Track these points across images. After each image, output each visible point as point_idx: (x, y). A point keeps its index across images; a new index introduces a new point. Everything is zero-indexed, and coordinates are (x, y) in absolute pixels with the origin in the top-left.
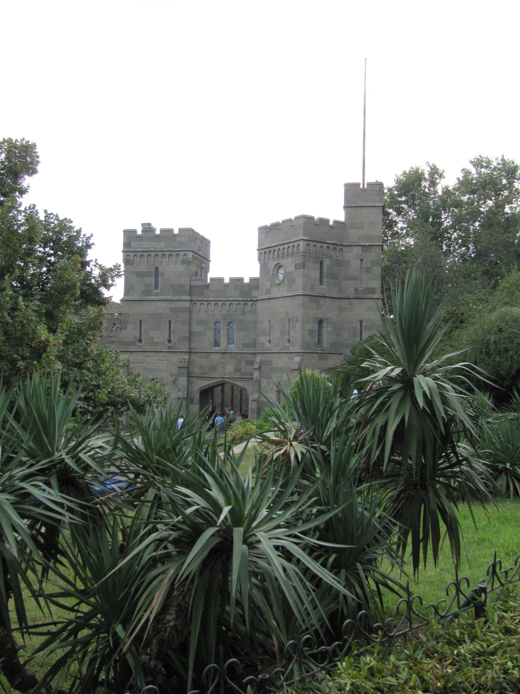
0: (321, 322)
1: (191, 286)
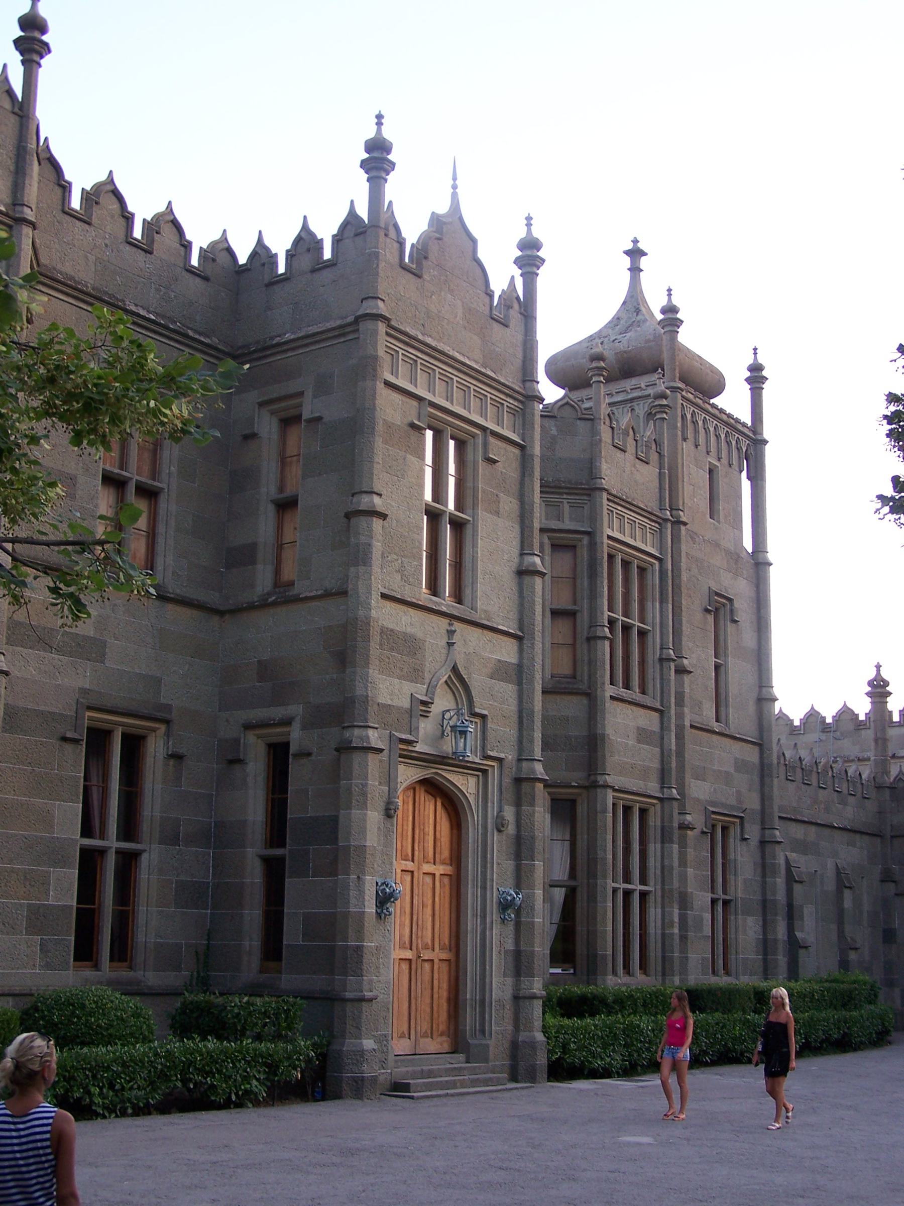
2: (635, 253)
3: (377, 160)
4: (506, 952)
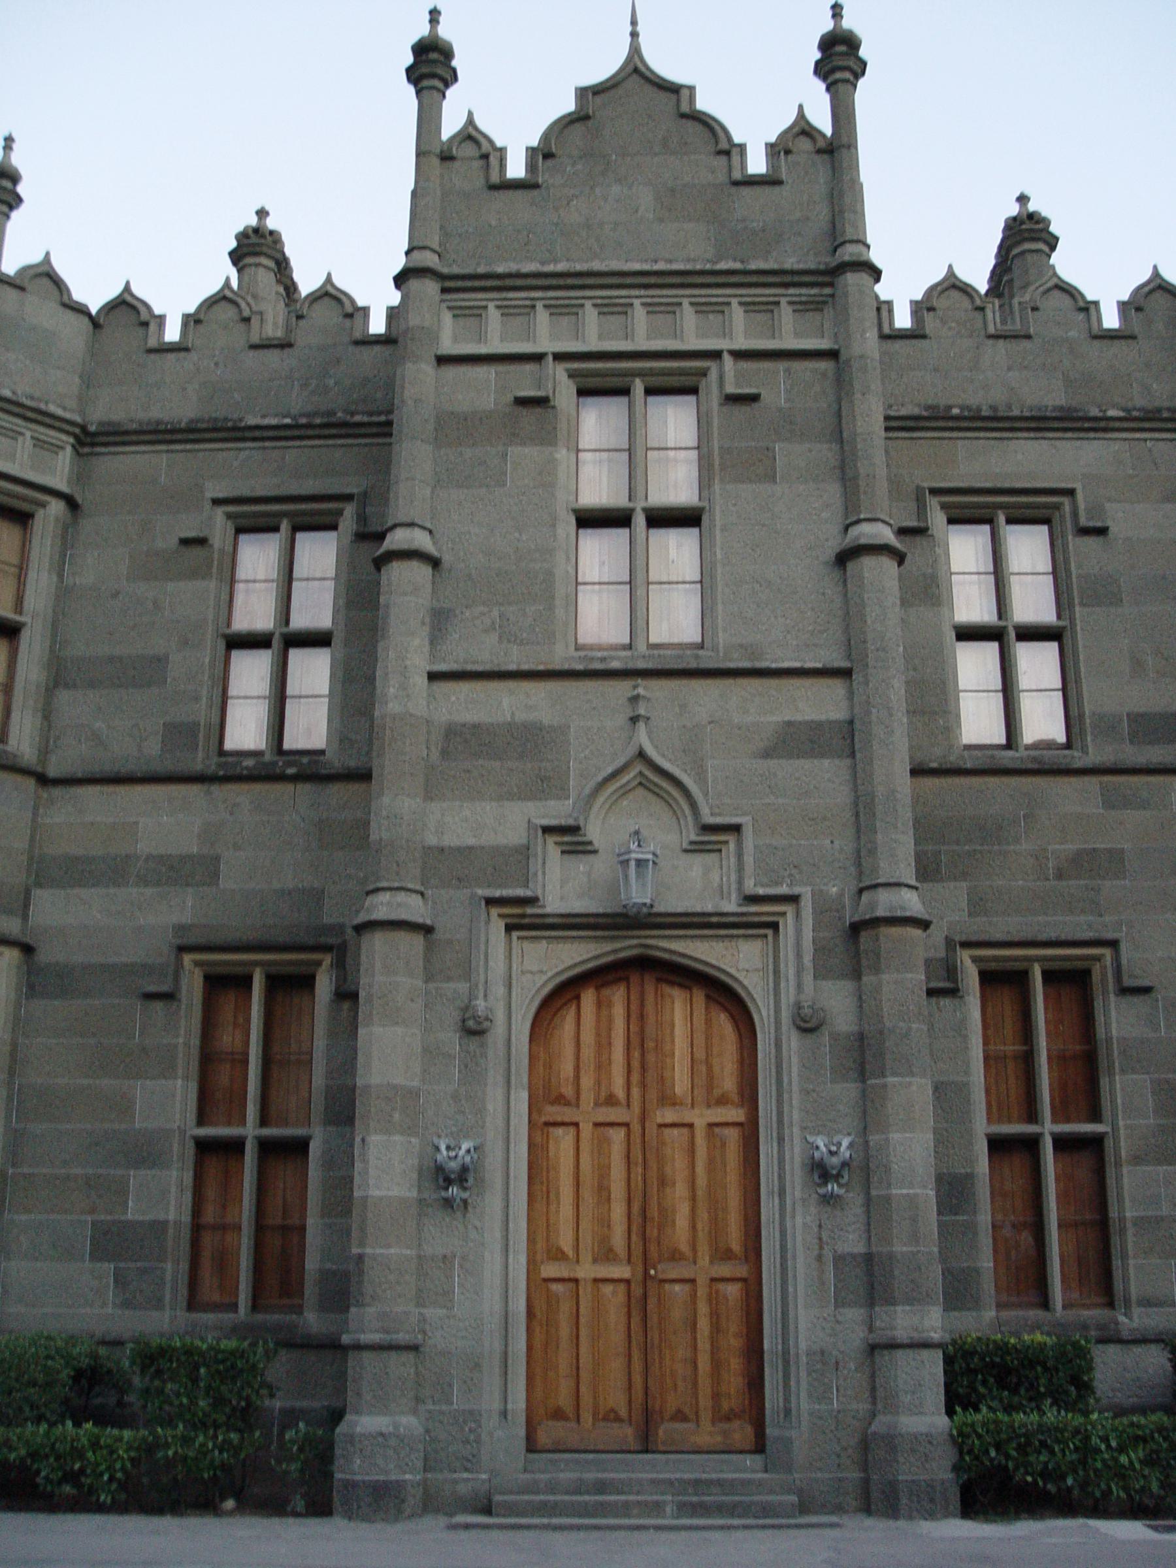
3: (431, 66)
4: (839, 1259)
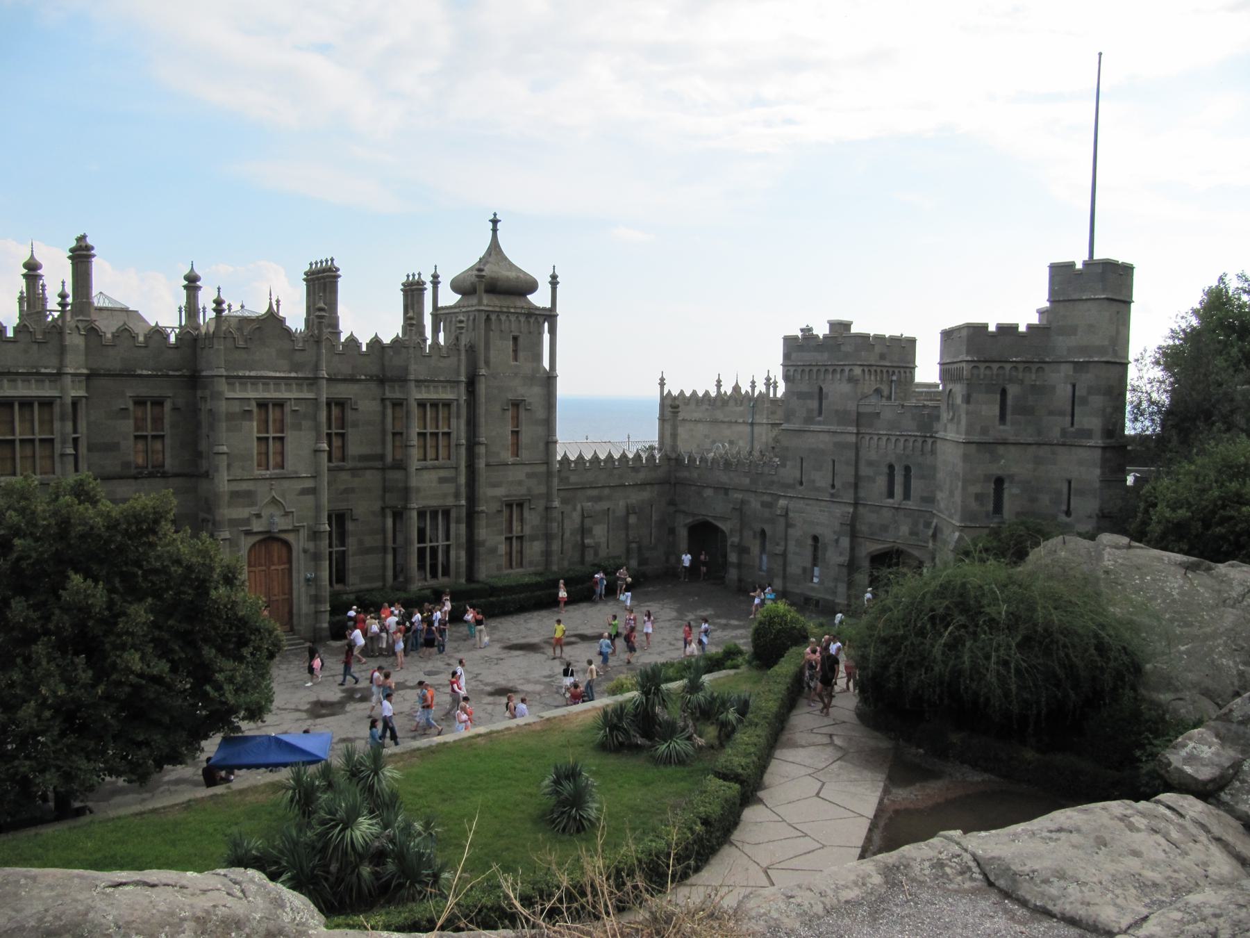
0: (999, 482)
1: (859, 414)
2: (495, 222)
